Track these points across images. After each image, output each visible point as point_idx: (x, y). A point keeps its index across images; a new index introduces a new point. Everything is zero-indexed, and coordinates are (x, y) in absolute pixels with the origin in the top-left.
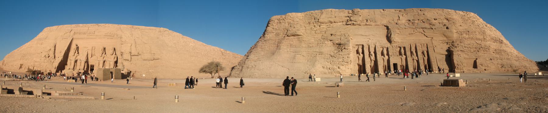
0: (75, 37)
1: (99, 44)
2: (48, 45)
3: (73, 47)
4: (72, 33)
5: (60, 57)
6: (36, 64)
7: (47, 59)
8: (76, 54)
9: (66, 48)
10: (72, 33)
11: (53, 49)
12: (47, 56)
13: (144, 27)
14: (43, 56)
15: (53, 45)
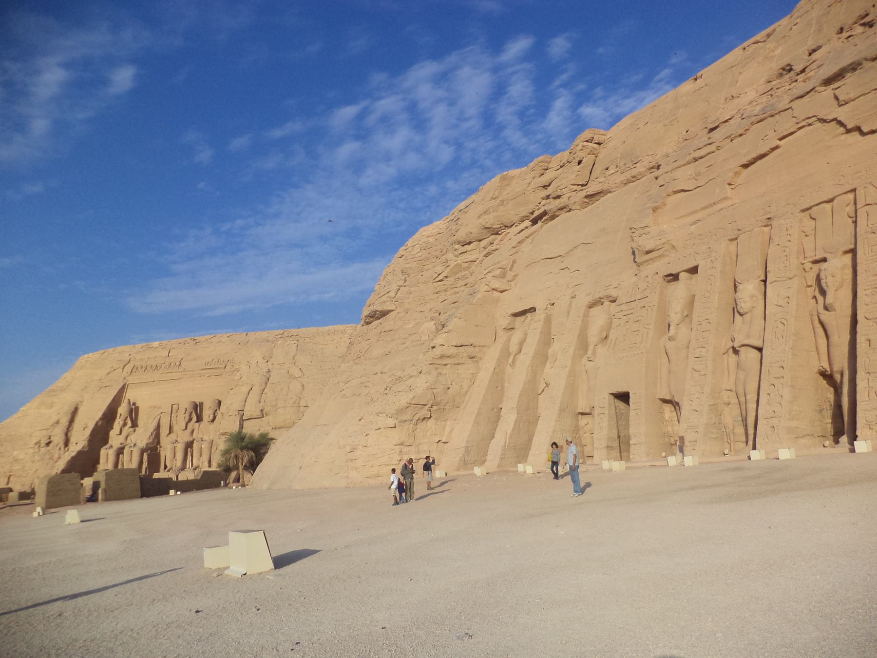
0: (131, 380)
1: (185, 392)
2: (59, 411)
3: (123, 410)
4: (128, 368)
5: (80, 440)
6: (16, 467)
7: (43, 450)
8: (126, 430)
9: (100, 414)
10: (128, 368)
11: (65, 421)
12: (44, 441)
13: (312, 330)
14: (34, 440)
15: (68, 408)
